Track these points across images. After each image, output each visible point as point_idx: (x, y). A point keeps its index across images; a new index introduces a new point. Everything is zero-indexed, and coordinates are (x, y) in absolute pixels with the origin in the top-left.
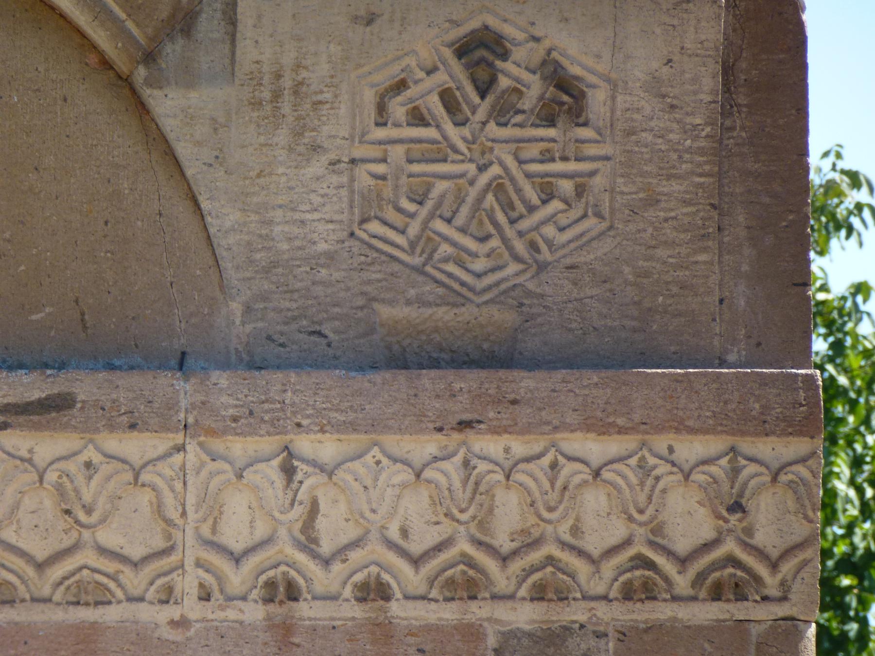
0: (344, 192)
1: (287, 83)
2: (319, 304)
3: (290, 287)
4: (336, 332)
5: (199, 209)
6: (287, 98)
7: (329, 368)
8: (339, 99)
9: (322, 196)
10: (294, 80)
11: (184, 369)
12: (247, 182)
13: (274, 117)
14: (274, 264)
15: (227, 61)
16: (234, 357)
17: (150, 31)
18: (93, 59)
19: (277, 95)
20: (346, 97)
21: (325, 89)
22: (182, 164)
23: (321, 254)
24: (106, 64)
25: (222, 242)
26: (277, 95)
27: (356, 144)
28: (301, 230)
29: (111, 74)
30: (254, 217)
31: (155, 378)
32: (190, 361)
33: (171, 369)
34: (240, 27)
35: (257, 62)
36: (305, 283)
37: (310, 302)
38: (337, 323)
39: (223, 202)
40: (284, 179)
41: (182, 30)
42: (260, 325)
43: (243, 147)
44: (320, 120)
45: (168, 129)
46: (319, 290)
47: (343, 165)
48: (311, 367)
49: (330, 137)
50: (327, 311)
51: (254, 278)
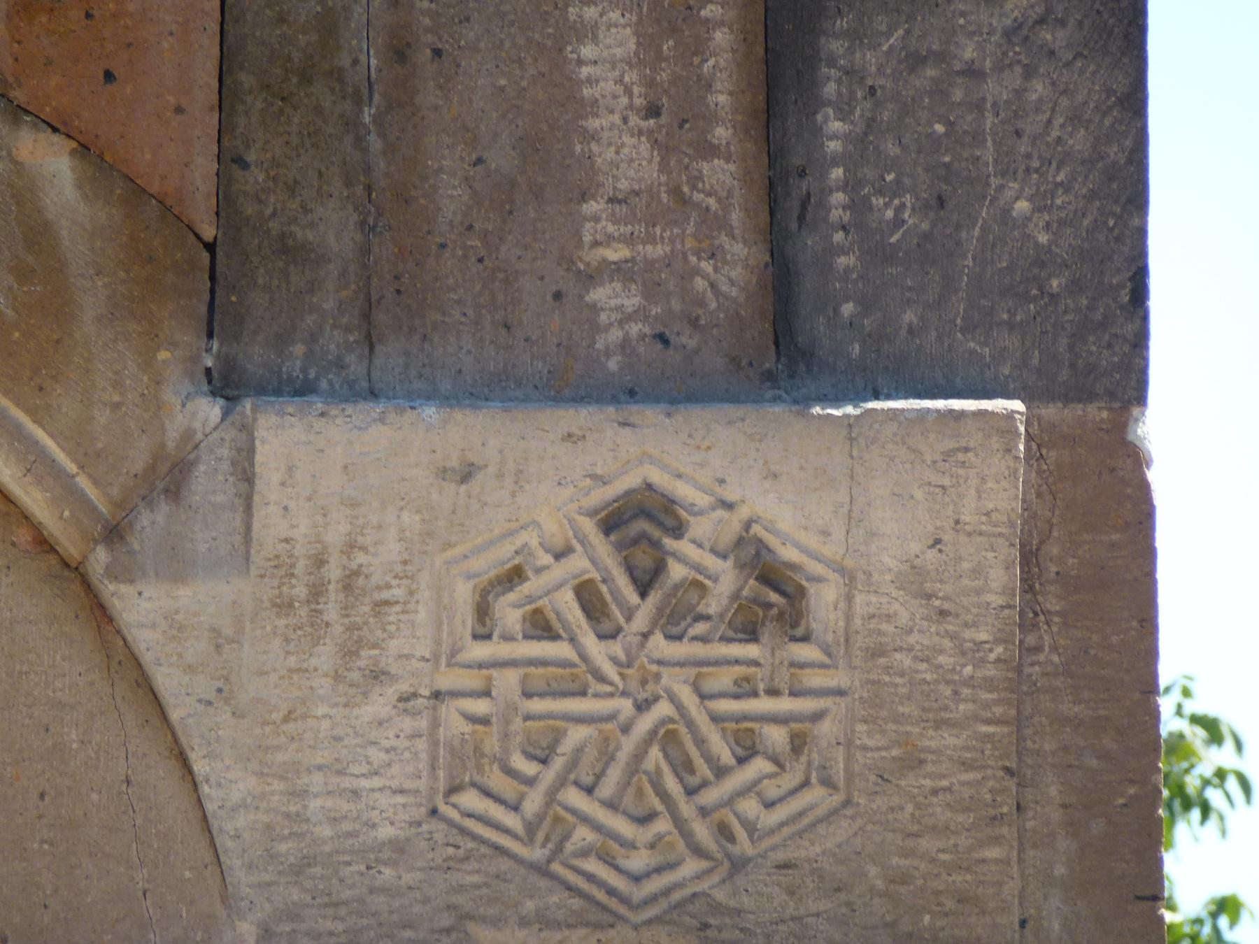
0: (422, 745)
1: (333, 572)
2: (381, 924)
3: (334, 898)
6: (333, 596)
8: (416, 597)
9: (387, 751)
10: (344, 568)
12: (268, 729)
13: (312, 625)
14: (308, 861)
15: (238, 539)
18: (23, 536)
19: (317, 592)
20: (427, 594)
21: (394, 582)
22: (164, 702)
23: (384, 844)
24: (44, 544)
25: (225, 826)
26: (317, 592)
27: (443, 668)
28: (352, 806)
29: (53, 560)
30: (277, 785)
34: (259, 485)
35: (287, 541)
36: (358, 892)
39: (228, 762)
40: (326, 724)
41: (166, 491)
43: (262, 673)
44: (384, 630)
45: (143, 646)
46: (379, 902)
47: (420, 701)
49: (400, 656)
51: (277, 883)
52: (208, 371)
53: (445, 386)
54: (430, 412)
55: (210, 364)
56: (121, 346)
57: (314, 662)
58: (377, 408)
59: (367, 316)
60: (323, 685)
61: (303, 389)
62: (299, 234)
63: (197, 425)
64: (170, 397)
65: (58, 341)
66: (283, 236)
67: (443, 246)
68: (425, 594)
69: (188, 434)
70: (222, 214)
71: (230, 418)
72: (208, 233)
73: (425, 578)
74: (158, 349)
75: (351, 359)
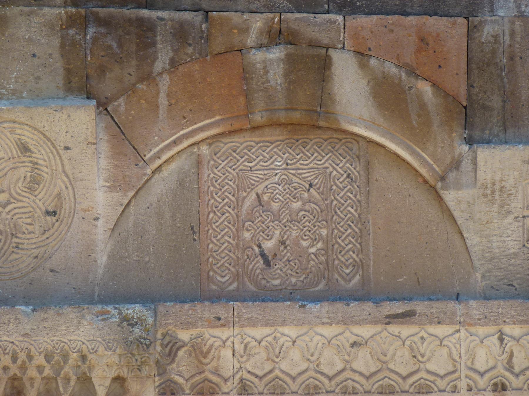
0: (521, 229)
1: (497, 187)
2: (512, 273)
3: (500, 267)
4: (518, 284)
5: (463, 237)
6: (497, 193)
7: (516, 299)
8: (518, 193)
9: (512, 231)
10: (500, 186)
11: (459, 300)
12: (482, 226)
13: (492, 200)
14: (493, 258)
15: (473, 179)
16: (478, 295)
17: (443, 168)
18: (420, 180)
19: (493, 192)
20: (521, 192)
21: (513, 189)
22: (456, 219)
23: (512, 254)
24: (426, 182)
25: (472, 250)
26: (493, 192)
27: (525, 210)
28: (504, 244)
29: (428, 185)
30: (485, 240)
31: (447, 303)
32: (461, 297)
33: (453, 300)
34: (478, 166)
35: (485, 179)
36: (506, 265)
37: (508, 273)
38: (519, 281)
39: (472, 234)
40: (496, 224)
41: (455, 168)
42: (488, 282)
43: (480, 212)
44: (510, 201)
45: (451, 206)
46: (511, 268)
47: (520, 218)
48: (509, 298)
49: (515, 207)
50: (514, 276)
51: (486, 264)
52: (465, 138)
53: (524, 140)
54: (521, 146)
55: (465, 136)
56: (444, 132)
57: (493, 209)
58: (507, 146)
59: (504, 123)
60: (496, 215)
61: (489, 142)
62: (487, 104)
63: (463, 151)
64: (456, 145)
65: (428, 132)
66: (483, 104)
67: (523, 105)
68: (520, 192)
69: (460, 154)
70: (468, 99)
71: (471, 149)
72: (465, 104)
73: (520, 188)
74: (453, 133)
75: (500, 134)
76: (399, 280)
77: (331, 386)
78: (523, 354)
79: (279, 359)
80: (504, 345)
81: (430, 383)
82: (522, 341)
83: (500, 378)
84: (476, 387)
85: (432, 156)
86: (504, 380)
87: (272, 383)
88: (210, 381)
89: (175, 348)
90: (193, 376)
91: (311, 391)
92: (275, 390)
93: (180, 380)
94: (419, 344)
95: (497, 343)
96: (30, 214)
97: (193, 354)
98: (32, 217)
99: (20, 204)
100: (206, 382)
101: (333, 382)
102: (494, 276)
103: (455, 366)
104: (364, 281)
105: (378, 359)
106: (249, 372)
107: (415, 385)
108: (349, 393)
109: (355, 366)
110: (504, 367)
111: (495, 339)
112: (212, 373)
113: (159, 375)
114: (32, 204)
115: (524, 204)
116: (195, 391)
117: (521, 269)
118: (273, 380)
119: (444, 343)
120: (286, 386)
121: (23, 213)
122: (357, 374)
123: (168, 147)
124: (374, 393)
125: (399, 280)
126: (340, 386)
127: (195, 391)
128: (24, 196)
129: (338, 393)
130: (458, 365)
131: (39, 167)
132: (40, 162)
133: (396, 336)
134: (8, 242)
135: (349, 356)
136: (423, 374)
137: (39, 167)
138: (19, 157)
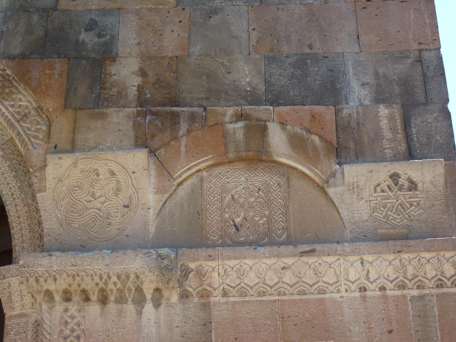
0: (369, 207)
1: (355, 185)
15: (343, 182)
17: (327, 177)
19: (353, 188)
25: (345, 219)
26: (353, 188)
30: (350, 213)
42: (353, 235)
46: (365, 227)
59: (357, 155)
60: (355, 200)
64: (333, 165)
66: (345, 146)
68: (367, 187)
69: (335, 170)
73: (367, 186)
75: (355, 160)
76: (307, 236)
77: (272, 291)
78: (374, 271)
79: (244, 277)
80: (364, 266)
81: (325, 288)
82: (373, 264)
83: (363, 284)
84: (350, 290)
85: (321, 171)
86: (365, 285)
87: (240, 291)
88: (207, 290)
89: (187, 272)
90: (198, 287)
91: (261, 295)
92: (241, 294)
93: (191, 290)
94: (318, 267)
95: (360, 265)
96: (116, 207)
97: (197, 276)
98: (117, 208)
99: (111, 202)
100: (205, 290)
101: (273, 289)
102: (356, 232)
103: (338, 279)
104: (288, 237)
105: (297, 276)
106: (227, 285)
107: (317, 289)
108: (282, 295)
109: (284, 280)
110: (365, 278)
111: (359, 263)
112: (207, 285)
113: (179, 287)
114: (117, 202)
115: (370, 194)
116: (199, 295)
117: (370, 228)
118: (241, 289)
119: (332, 266)
120: (247, 292)
121: (112, 207)
122: (286, 285)
123: (185, 171)
124: (295, 294)
125: (307, 236)
126: (277, 291)
127: (199, 295)
128: (112, 198)
129: (275, 295)
130: (340, 278)
131: (120, 183)
132: (120, 180)
133: (306, 263)
134: (105, 221)
135: (281, 274)
136: (321, 284)
137: (120, 183)
138: (110, 178)
